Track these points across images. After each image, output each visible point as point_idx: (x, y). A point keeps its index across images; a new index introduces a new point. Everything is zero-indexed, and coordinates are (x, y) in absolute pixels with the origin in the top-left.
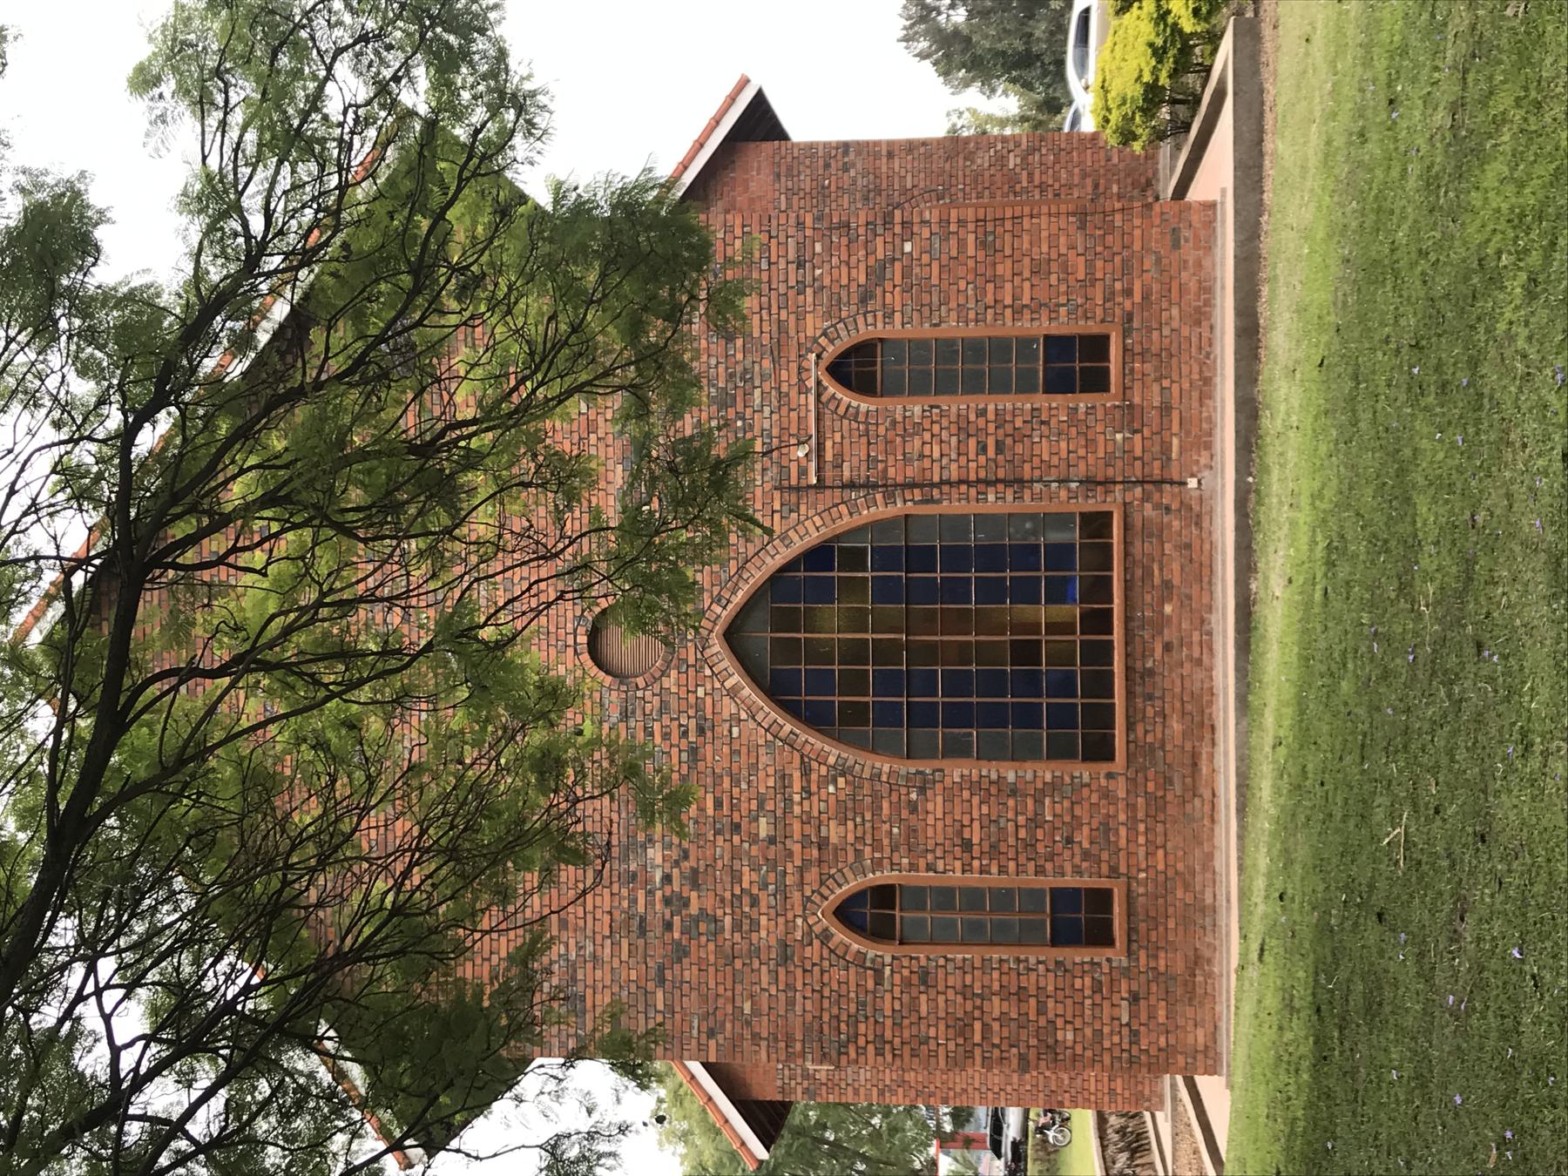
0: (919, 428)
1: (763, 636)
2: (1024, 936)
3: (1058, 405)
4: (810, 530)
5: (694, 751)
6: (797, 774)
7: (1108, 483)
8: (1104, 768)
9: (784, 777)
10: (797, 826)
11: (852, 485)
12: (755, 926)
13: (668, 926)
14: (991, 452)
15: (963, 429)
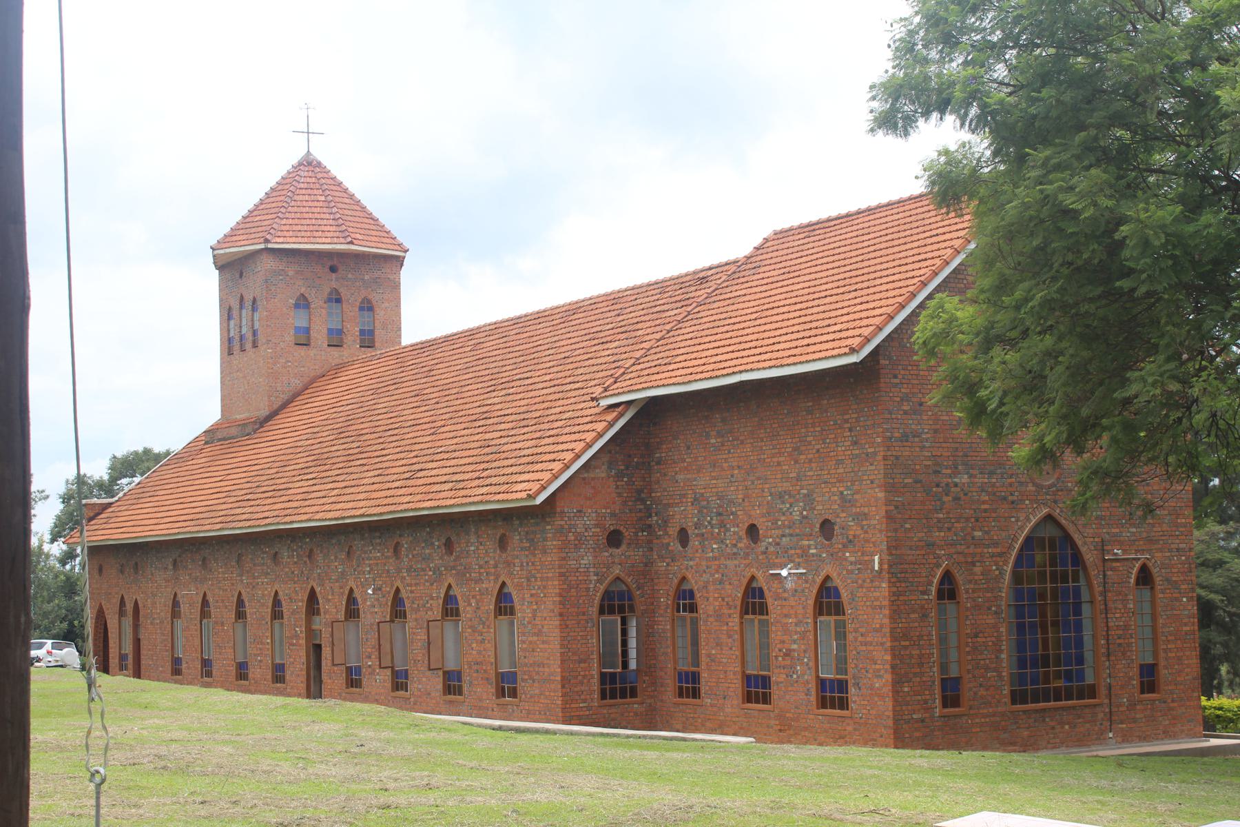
0: (1125, 607)
1: (1050, 532)
2: (944, 668)
3: (1135, 672)
4: (1089, 556)
5: (1005, 498)
6: (999, 550)
7: (1109, 696)
8: (1008, 700)
9: (995, 544)
10: (979, 550)
11: (1105, 575)
12: (940, 530)
13: (937, 486)
14: (1118, 641)
15: (1126, 627)
